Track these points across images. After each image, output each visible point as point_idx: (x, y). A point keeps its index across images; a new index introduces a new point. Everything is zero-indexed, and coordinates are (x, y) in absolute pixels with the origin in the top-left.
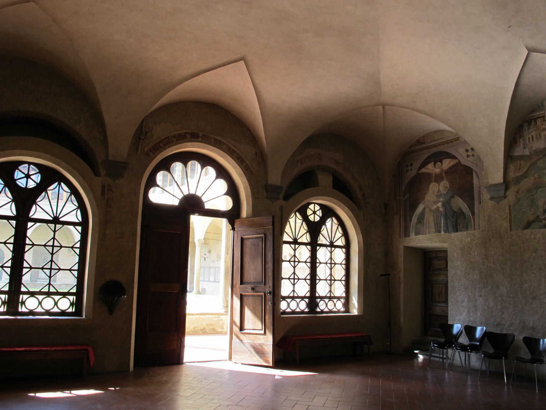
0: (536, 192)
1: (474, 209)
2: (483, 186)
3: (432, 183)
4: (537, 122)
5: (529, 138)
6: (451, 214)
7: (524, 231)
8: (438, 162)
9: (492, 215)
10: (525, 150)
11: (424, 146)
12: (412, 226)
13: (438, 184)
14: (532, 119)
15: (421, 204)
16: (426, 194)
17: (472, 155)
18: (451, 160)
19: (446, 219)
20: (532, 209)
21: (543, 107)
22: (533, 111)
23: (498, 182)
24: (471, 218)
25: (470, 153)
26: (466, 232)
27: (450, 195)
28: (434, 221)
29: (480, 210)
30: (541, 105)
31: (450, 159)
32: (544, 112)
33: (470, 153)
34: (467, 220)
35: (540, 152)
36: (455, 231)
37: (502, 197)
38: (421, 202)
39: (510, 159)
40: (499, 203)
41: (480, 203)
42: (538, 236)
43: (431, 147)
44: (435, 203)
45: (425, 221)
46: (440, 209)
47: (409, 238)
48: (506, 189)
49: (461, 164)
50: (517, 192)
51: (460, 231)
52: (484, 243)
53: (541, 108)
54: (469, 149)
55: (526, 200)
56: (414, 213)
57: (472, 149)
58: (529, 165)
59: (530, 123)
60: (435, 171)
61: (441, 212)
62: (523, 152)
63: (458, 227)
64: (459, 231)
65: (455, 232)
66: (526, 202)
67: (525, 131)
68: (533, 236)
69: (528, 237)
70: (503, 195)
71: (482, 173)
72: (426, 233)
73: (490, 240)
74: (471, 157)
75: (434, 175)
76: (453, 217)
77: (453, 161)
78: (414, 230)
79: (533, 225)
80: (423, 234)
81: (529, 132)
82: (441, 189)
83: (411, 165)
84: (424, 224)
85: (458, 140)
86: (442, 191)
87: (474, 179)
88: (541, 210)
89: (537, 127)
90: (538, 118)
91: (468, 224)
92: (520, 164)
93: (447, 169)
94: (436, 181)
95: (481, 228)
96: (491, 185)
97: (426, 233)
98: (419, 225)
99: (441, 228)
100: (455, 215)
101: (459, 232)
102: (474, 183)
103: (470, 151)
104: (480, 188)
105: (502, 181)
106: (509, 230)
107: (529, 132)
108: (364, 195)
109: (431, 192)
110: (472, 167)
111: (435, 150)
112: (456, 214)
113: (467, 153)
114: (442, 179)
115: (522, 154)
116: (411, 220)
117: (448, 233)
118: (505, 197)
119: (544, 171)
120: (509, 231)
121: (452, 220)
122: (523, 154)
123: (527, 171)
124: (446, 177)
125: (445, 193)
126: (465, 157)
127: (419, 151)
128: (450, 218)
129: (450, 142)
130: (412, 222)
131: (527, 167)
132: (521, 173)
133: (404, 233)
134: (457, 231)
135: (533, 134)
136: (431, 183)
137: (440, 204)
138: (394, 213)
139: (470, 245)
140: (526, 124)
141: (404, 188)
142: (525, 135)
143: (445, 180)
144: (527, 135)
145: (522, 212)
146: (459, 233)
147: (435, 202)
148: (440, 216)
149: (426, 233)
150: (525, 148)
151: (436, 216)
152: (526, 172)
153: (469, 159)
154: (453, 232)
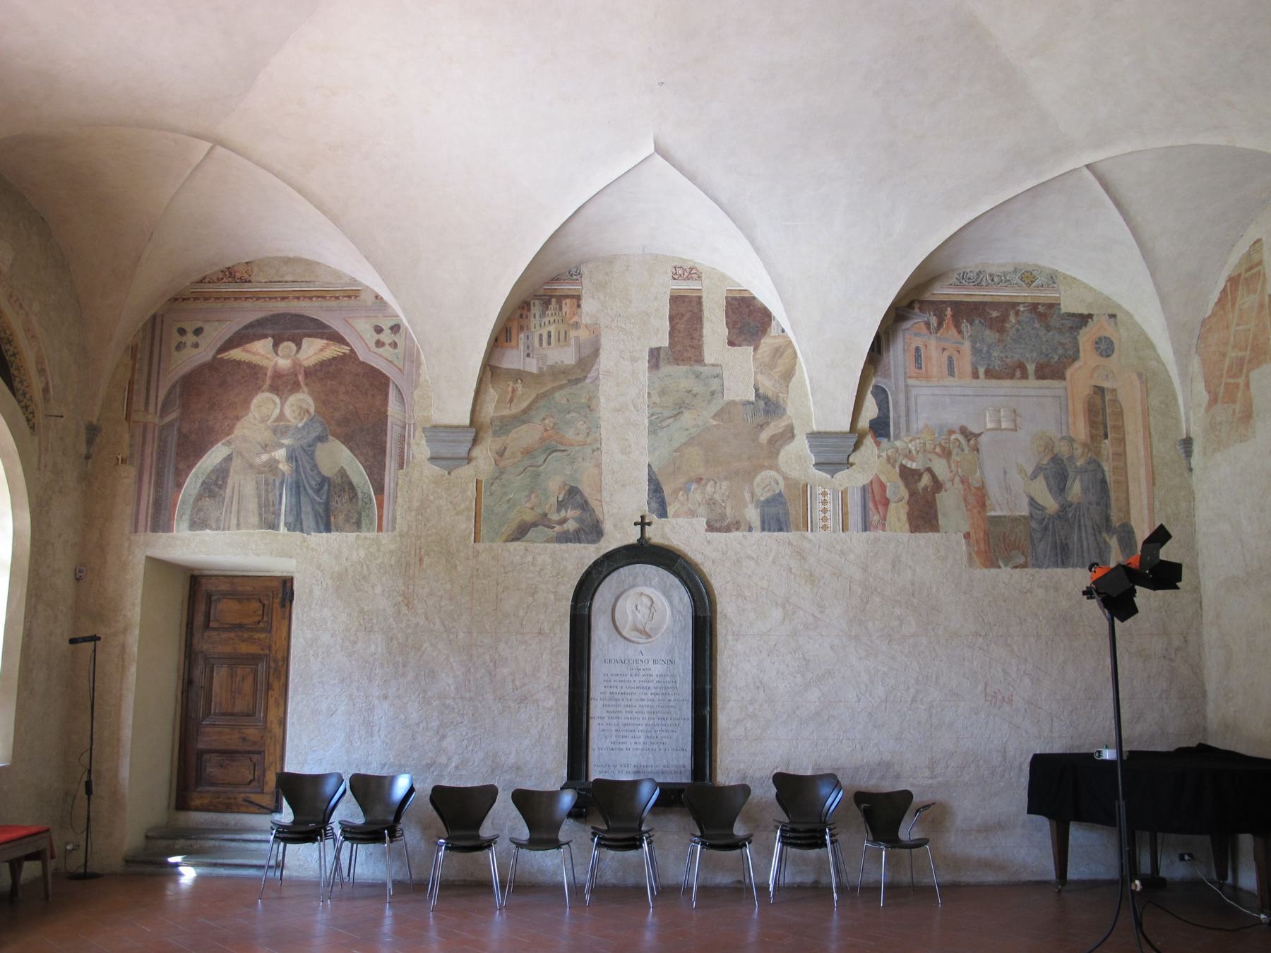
0: (545, 461)
1: (383, 479)
2: (412, 426)
3: (263, 392)
4: (563, 306)
5: (541, 336)
6: (313, 483)
7: (508, 544)
8: (288, 340)
9: (431, 498)
10: (527, 358)
11: (246, 288)
12: (183, 501)
13: (281, 398)
14: (551, 297)
15: (220, 444)
16: (238, 418)
17: (390, 344)
18: (327, 344)
19: (298, 494)
20: (533, 496)
21: (578, 277)
22: (556, 279)
23: (455, 422)
25: (386, 337)
26: (355, 534)
27: (314, 435)
28: (259, 497)
29: (400, 481)
30: (575, 270)
31: (325, 341)
32: (580, 287)
34: (360, 502)
35: (564, 373)
36: (322, 527)
37: (463, 459)
38: (222, 440)
39: (490, 373)
40: (452, 474)
41: (401, 467)
42: (540, 559)
43: (272, 297)
44: (265, 447)
45: (228, 491)
46: (281, 466)
47: (171, 534)
48: (475, 441)
49: (357, 359)
50: (501, 454)
51: (337, 531)
52: (404, 565)
53: (575, 277)
54: (384, 328)
55: (519, 475)
56: (190, 467)
57: (396, 328)
58: (534, 396)
59: (546, 303)
60: (276, 364)
61: (284, 474)
62: (524, 363)
64: (333, 528)
65: (320, 532)
66: (519, 478)
67: (535, 318)
68: (530, 559)
69: (517, 559)
70: (466, 455)
71: (412, 393)
72: (227, 526)
73: (421, 560)
74: (387, 347)
75: (269, 373)
76: (318, 491)
77: (333, 348)
78: (188, 512)
79: (531, 534)
80: (218, 528)
81: (543, 324)
82: (287, 411)
83: (198, 331)
84: (223, 502)
85: (356, 297)
86: (292, 420)
87: (390, 403)
88: (553, 500)
89: (562, 316)
90: (567, 297)
91: (363, 514)
92: (514, 391)
93: (314, 366)
94: (274, 389)
95: (397, 527)
96: (435, 427)
97: (227, 526)
98: (207, 503)
99: (279, 515)
100: (326, 487)
101: (333, 533)
102: (389, 413)
103: (387, 331)
104: (404, 428)
105: (467, 422)
106: (473, 538)
107: (543, 324)
108: (46, 390)
109: (255, 418)
110: (387, 374)
111: (281, 307)
112: (329, 486)
113: (376, 337)
114: (296, 387)
115: (522, 369)
116: (179, 485)
117: (298, 533)
118: (469, 459)
119: (568, 416)
120: (473, 542)
121: (316, 498)
122: (524, 368)
123: (529, 408)
124: (306, 385)
125: (300, 425)
126: (372, 345)
127: (229, 298)
128: (310, 491)
129: (331, 297)
130: (183, 491)
131: (531, 399)
132: (515, 410)
133: (149, 519)
134: (328, 530)
135: (552, 328)
136: (257, 394)
137: (281, 454)
138: (120, 457)
139: (365, 566)
140: (537, 302)
141: (163, 393)
142: (532, 328)
143: (303, 392)
144: (538, 327)
145: (509, 501)
146: (334, 536)
147: (266, 445)
149: (229, 526)
150: (528, 355)
151: (267, 483)
152: (525, 411)
153: (381, 350)
154: (315, 532)
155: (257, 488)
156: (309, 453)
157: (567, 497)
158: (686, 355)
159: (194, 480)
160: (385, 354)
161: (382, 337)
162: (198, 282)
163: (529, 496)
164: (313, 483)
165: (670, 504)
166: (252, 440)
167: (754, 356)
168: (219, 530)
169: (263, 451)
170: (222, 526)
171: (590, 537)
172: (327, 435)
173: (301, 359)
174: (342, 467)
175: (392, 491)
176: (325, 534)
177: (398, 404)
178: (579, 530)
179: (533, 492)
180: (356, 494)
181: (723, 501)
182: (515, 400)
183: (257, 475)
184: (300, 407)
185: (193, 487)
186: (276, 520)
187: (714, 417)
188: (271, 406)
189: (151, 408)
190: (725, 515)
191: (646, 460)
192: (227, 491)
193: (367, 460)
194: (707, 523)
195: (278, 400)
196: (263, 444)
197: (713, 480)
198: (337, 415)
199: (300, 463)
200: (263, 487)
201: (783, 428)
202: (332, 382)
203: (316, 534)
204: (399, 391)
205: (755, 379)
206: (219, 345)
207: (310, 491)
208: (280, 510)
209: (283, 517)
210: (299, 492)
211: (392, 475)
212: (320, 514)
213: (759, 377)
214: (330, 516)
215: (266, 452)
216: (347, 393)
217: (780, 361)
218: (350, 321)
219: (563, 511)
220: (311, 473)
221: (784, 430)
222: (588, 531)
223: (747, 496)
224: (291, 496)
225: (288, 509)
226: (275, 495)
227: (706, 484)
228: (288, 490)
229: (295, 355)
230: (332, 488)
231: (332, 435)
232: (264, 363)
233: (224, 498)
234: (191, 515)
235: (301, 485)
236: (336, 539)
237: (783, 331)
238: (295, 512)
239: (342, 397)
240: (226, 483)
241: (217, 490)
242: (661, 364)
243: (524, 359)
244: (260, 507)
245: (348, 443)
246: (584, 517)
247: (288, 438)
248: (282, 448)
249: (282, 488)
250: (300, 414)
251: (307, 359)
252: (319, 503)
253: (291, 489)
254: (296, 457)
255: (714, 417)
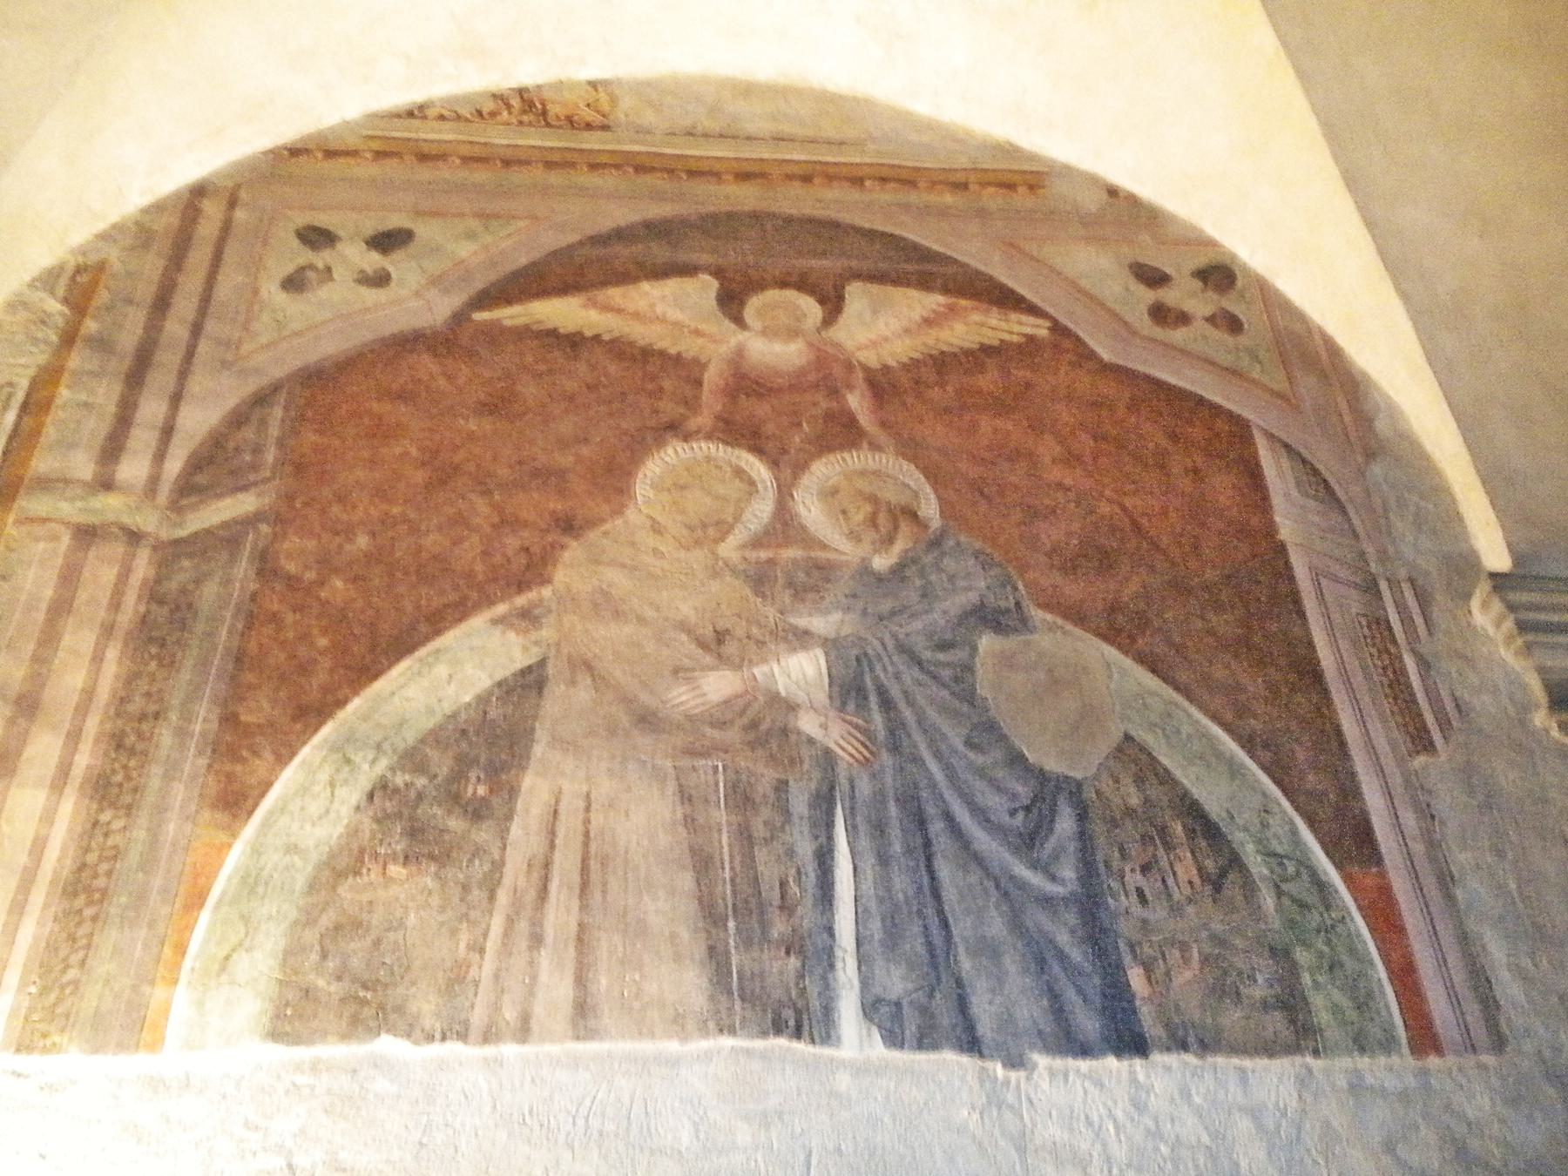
1: (1350, 790)
2: (1406, 587)
8: (783, 284)
13: (774, 464)
15: (478, 621)
17: (1211, 320)
18: (951, 309)
24: (1321, 886)
28: (703, 863)
33: (1184, 295)
34: (1268, 901)
45: (524, 835)
46: (808, 724)
60: (740, 352)
61: (828, 759)
63: (1136, 978)
74: (1199, 326)
76: (1028, 842)
77: (976, 317)
82: (810, 510)
86: (845, 545)
91: (1302, 956)
97: (510, 1014)
100: (1065, 824)
101: (1158, 1057)
104: (1370, 588)
109: (656, 528)
112: (1082, 817)
113: (1148, 296)
117: (951, 1060)
121: (1022, 871)
128: (983, 841)
147: (721, 636)
148: (799, 803)
151: (741, 798)
153: (1179, 335)
155: (689, 821)
156: (946, 673)
159: (323, 777)
160: (1198, 347)
161: (1170, 296)
162: (399, 116)
164: (994, 802)
166: (650, 613)
168: (463, 1036)
169: (708, 659)
170: (478, 1017)
172: (1018, 604)
173: (849, 345)
174: (1128, 738)
175: (1418, 848)
176: (1111, 1061)
177: (1312, 503)
180: (1235, 861)
183: (686, 762)
184: (873, 499)
185: (314, 808)
186: (813, 990)
188: (734, 489)
189: (133, 469)
192: (516, 830)
193: (1242, 711)
195: (759, 470)
196: (708, 632)
198: (1051, 533)
199: (908, 714)
200: (721, 815)
202: (999, 423)
203: (1059, 1063)
204: (1304, 461)
206: (479, 284)
207: (983, 841)
208: (830, 931)
209: (847, 971)
210: (927, 844)
211: (1396, 781)
212: (1062, 956)
214: (1120, 966)
215: (723, 661)
216: (1071, 459)
218: (1033, 249)
220: (979, 759)
224: (884, 860)
225: (875, 927)
226: (791, 853)
228: (863, 828)
229: (818, 331)
230: (1098, 828)
231: (1046, 606)
232: (688, 347)
233: (498, 865)
234: (291, 956)
235: (931, 810)
236: (1186, 1094)
238: (914, 944)
239: (1055, 474)
240: (513, 792)
241: (455, 824)
244: (711, 915)
245: (1132, 639)
247: (827, 612)
248: (805, 647)
249: (830, 825)
250: (873, 521)
251: (874, 344)
252: (1047, 901)
253: (879, 828)
254: (882, 692)
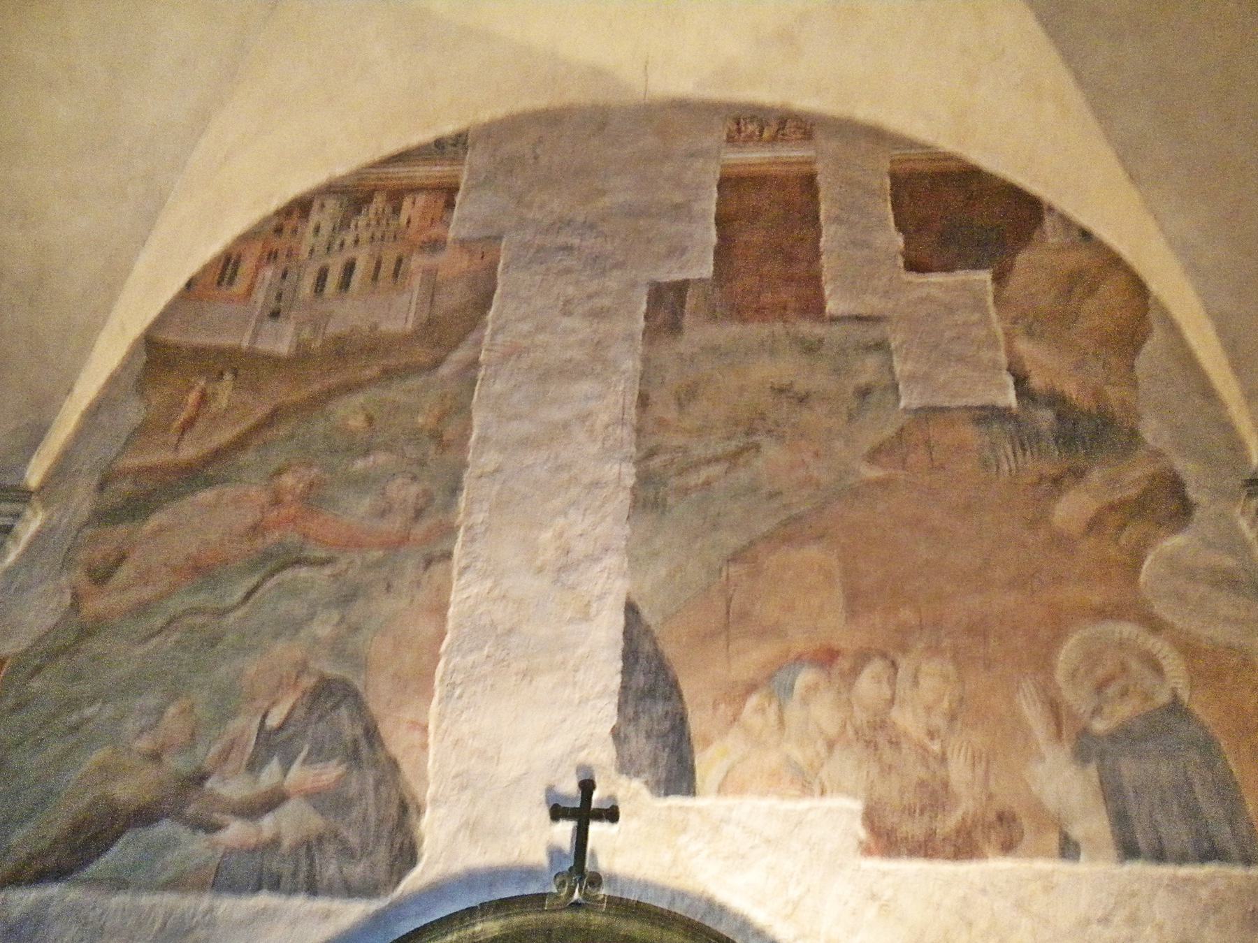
0: (249, 595)
10: (268, 325)
20: (172, 710)
66: (139, 651)
92: (204, 399)
131: (250, 421)
157: (301, 712)
158: (767, 298)
163: (161, 711)
165: (707, 742)
167: (997, 298)
171: (357, 871)
178: (320, 839)
179: (174, 696)
181: (932, 734)
182: (200, 425)
187: (873, 456)
190: (946, 785)
191: (620, 588)
194: (871, 817)
197: (884, 656)
201: (1144, 484)
205: (1010, 352)
213: (1024, 346)
217: (1091, 305)
219: (274, 766)
221: (1146, 492)
222: (354, 840)
223: (1033, 714)
227: (855, 671)
237: (1086, 234)
242: (687, 321)
243: (260, 321)
246: (353, 789)
255: (873, 456)
